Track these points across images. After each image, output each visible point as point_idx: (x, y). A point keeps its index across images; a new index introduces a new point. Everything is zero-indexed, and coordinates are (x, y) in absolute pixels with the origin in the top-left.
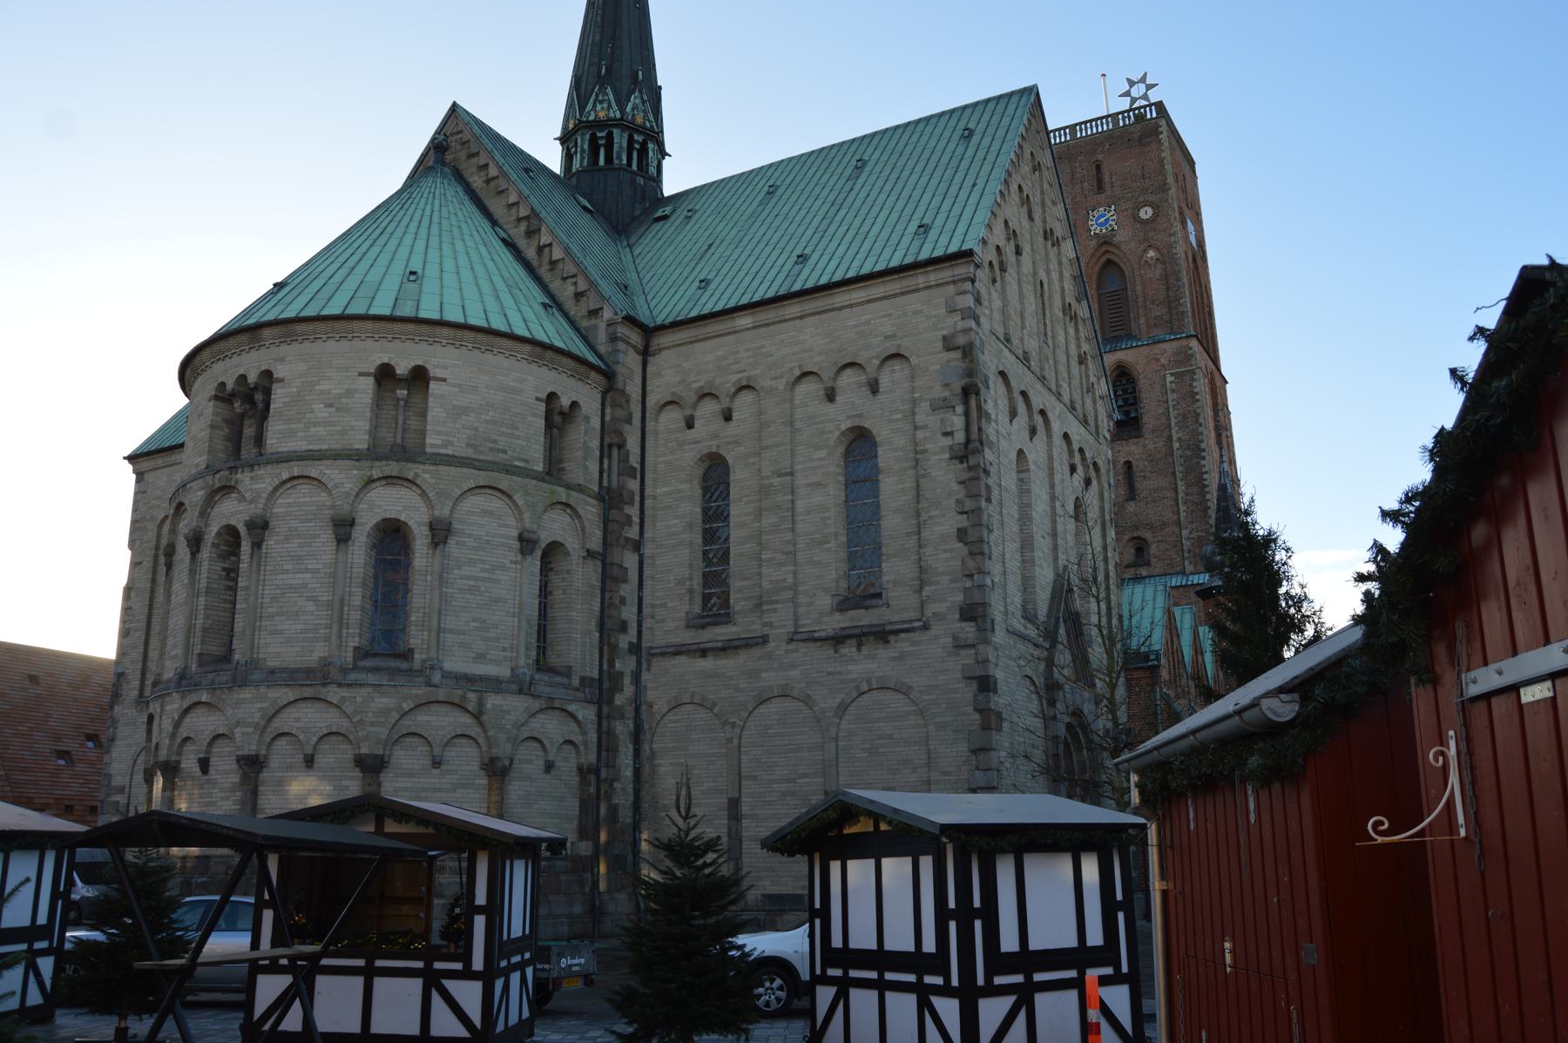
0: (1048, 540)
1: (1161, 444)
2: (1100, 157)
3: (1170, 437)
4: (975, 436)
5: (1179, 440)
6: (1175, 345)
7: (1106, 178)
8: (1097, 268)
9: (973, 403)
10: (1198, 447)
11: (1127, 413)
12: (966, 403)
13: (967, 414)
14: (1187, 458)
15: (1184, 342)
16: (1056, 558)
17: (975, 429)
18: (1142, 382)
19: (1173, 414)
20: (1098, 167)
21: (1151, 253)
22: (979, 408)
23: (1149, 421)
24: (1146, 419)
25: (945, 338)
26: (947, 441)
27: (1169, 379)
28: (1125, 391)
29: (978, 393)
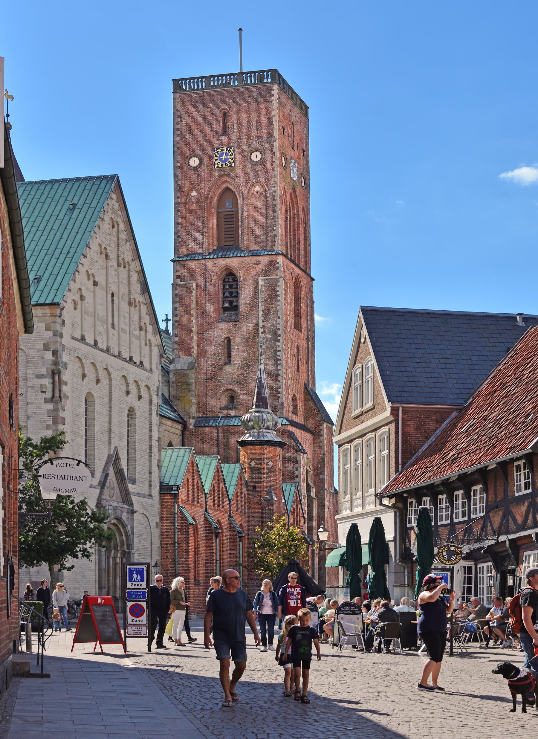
0: (106, 434)
1: (250, 329)
2: (226, 106)
3: (258, 324)
4: (57, 394)
5: (264, 326)
6: (267, 258)
7: (229, 124)
8: (218, 192)
9: (57, 378)
10: (276, 333)
11: (231, 303)
12: (53, 377)
13: (53, 383)
14: (267, 340)
15: (273, 258)
16: (110, 443)
17: (57, 391)
18: (242, 283)
19: (261, 308)
20: (225, 114)
21: (257, 188)
22: (60, 379)
23: (244, 311)
24: (241, 308)
25: (44, 344)
26: (44, 396)
27: (261, 283)
28: (231, 286)
29: (60, 373)
